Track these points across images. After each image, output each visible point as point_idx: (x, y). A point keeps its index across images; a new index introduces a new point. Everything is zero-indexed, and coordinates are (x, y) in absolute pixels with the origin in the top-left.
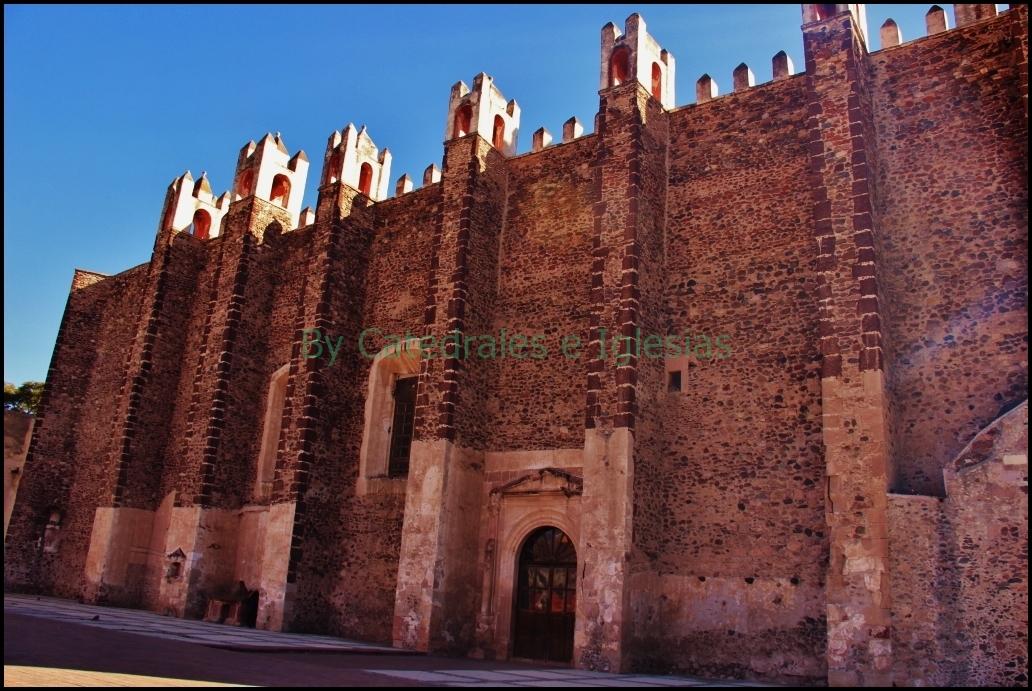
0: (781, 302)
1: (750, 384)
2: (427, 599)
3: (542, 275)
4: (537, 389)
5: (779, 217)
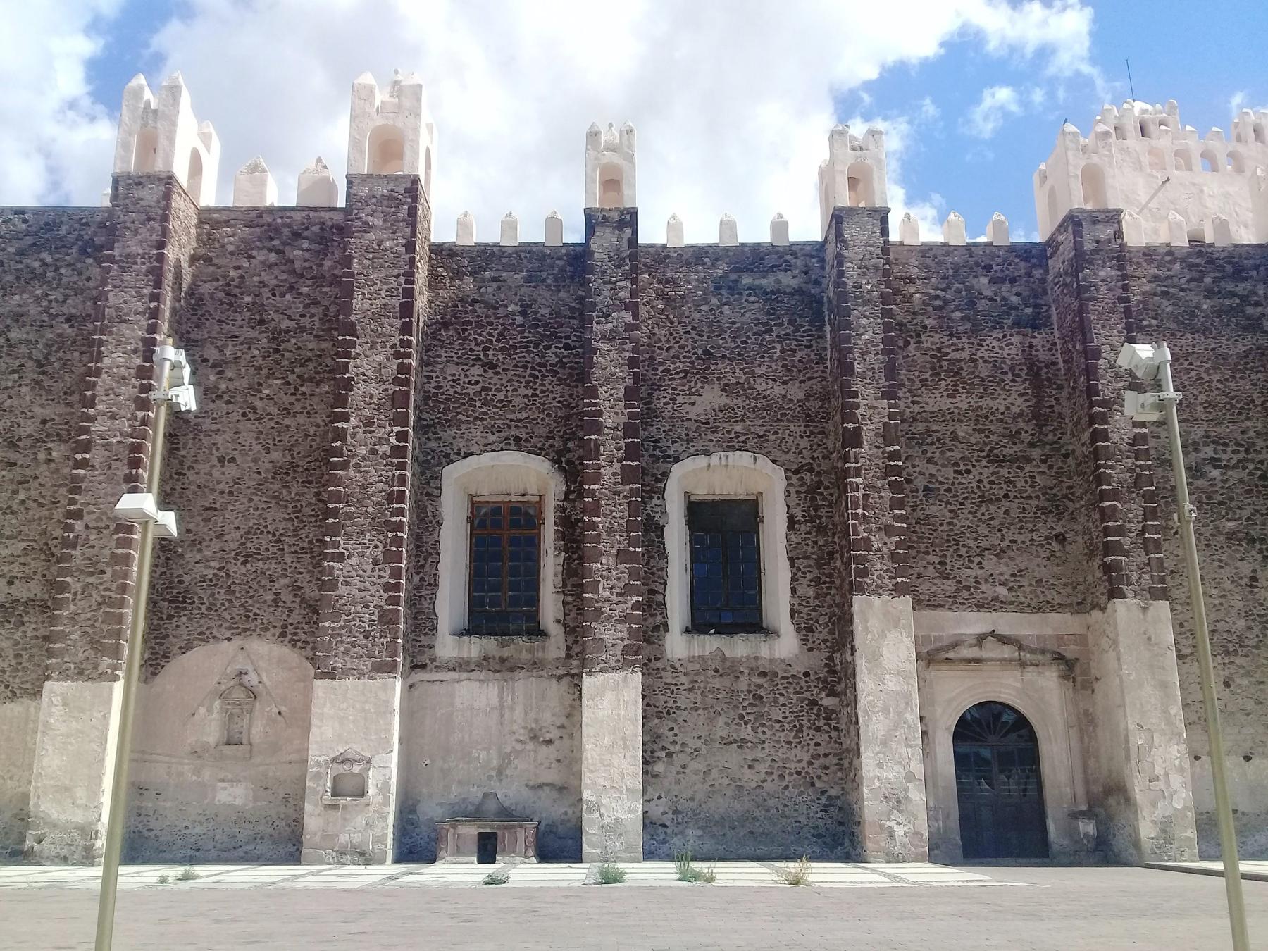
0: (1242, 481)
1: (1220, 561)
2: (917, 796)
3: (938, 401)
4: (955, 539)
5: (1233, 394)
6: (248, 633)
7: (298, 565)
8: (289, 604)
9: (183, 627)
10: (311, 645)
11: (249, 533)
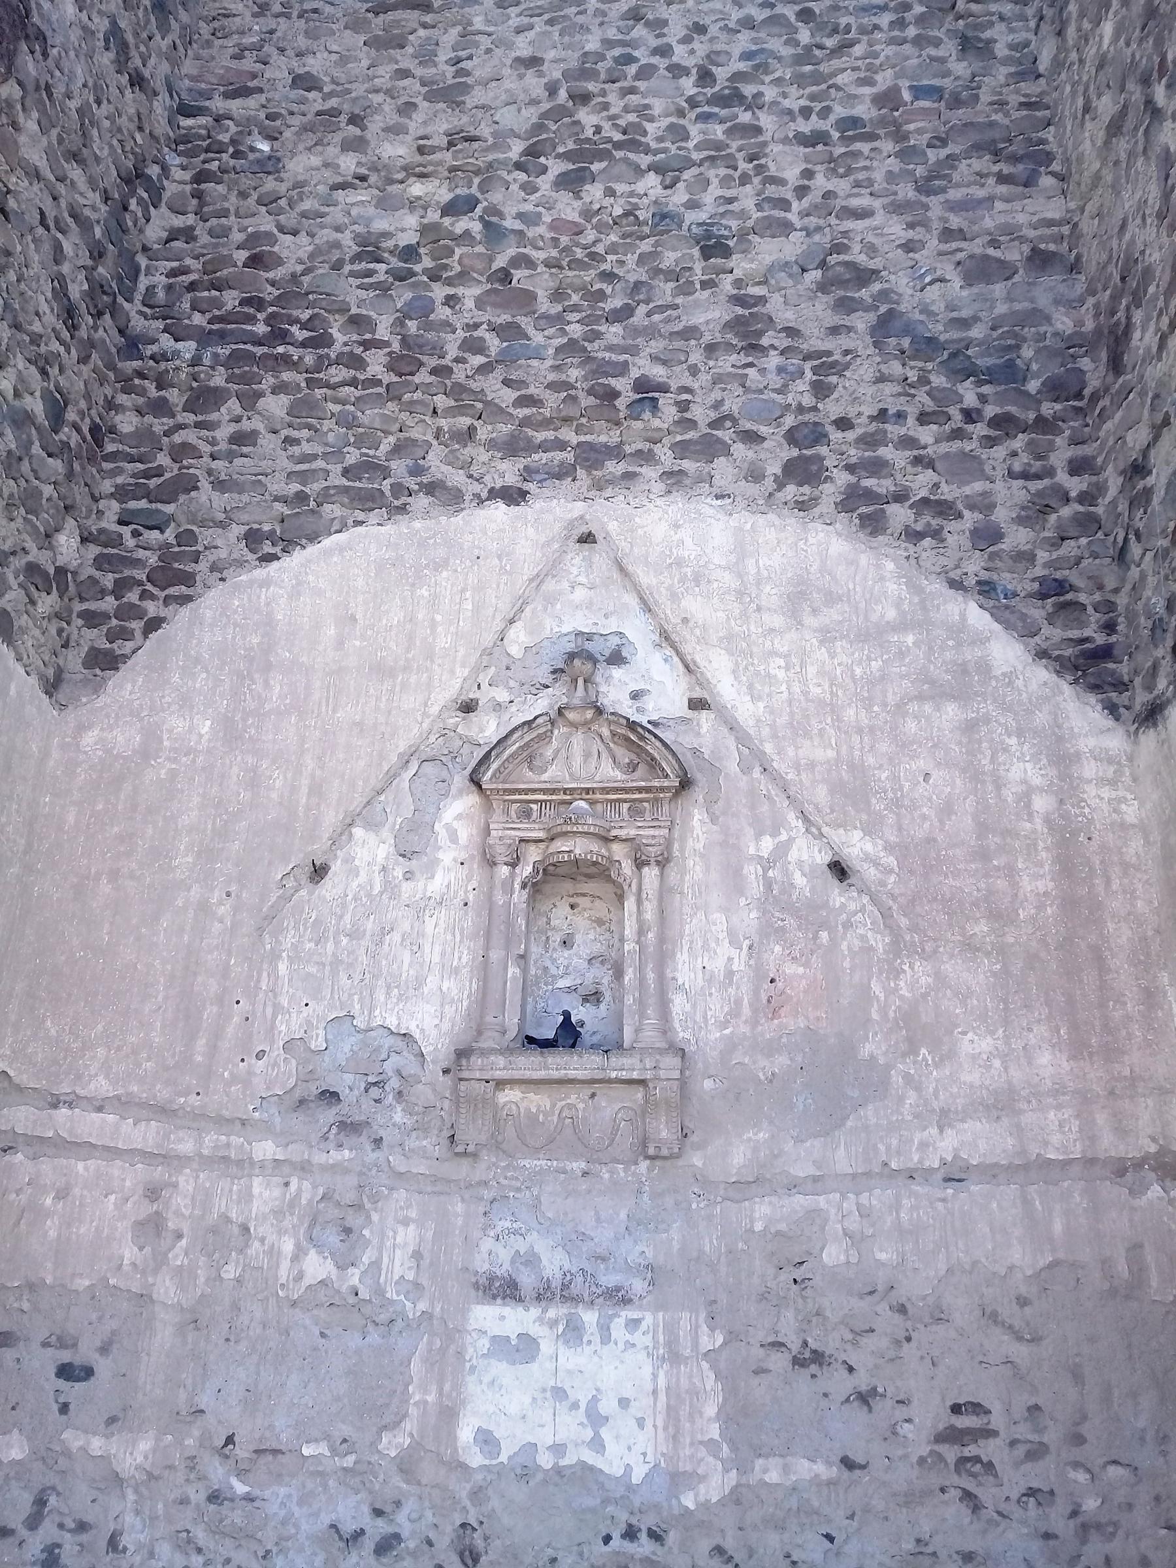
6: (614, 468)
7: (841, 186)
8: (815, 341)
9: (268, 443)
10: (970, 518)
11: (585, 73)
